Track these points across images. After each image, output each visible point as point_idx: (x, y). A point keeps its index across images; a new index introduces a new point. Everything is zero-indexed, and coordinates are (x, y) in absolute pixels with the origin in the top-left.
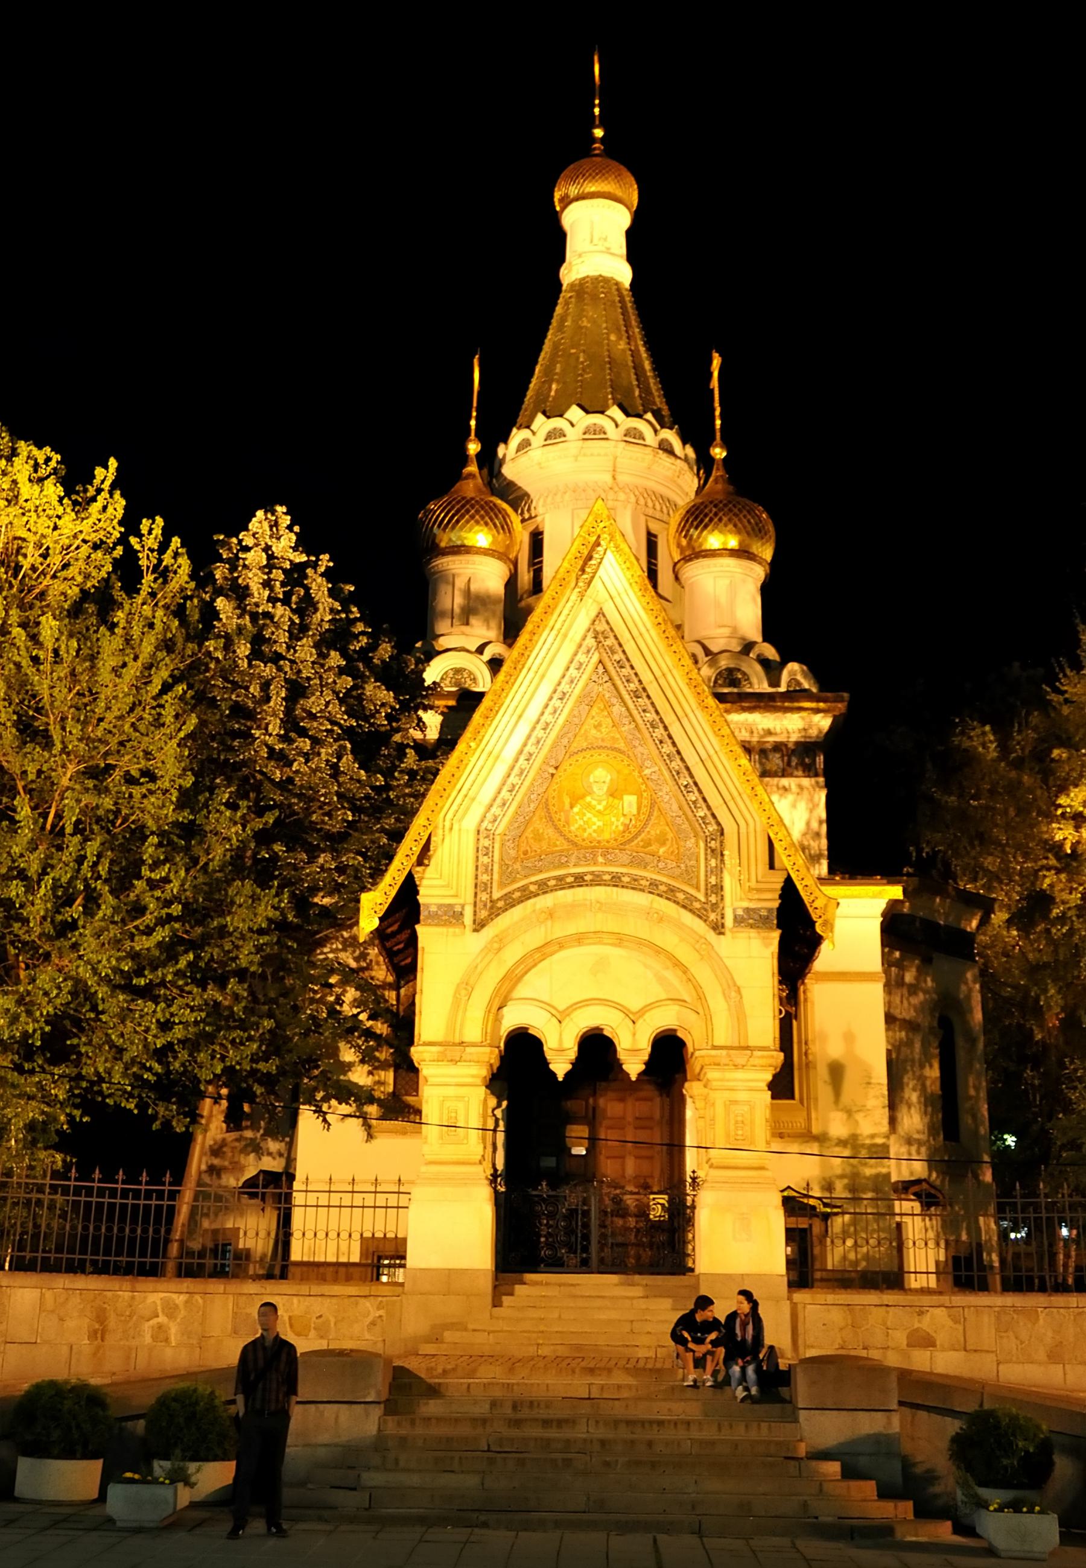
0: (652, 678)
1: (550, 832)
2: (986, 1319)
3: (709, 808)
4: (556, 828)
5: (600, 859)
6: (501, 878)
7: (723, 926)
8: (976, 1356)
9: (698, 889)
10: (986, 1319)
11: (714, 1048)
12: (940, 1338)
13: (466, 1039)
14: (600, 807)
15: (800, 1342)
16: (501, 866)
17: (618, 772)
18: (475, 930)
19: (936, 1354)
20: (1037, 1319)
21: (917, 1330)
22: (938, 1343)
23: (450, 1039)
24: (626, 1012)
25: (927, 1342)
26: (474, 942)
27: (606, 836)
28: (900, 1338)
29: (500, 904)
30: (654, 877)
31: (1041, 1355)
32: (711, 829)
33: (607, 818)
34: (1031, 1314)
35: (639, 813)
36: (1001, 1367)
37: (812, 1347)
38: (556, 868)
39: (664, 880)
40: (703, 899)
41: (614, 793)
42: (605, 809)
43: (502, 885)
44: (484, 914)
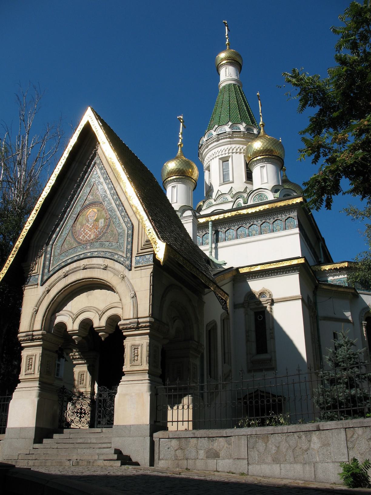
0: (110, 170)
1: (72, 241)
2: (243, 442)
3: (129, 218)
4: (75, 239)
5: (88, 247)
6: (53, 262)
7: (131, 266)
8: (238, 462)
9: (123, 252)
10: (243, 442)
11: (124, 320)
12: (222, 454)
13: (34, 329)
14: (91, 227)
15: (156, 457)
16: (54, 258)
17: (98, 211)
18: (42, 285)
19: (219, 461)
20: (268, 441)
21: (210, 450)
22: (221, 455)
23: (28, 330)
24: (97, 310)
25: (216, 455)
26: (41, 290)
27: (92, 237)
28: (202, 453)
29: (51, 273)
30: (107, 250)
31: (269, 459)
32: (129, 225)
33: (93, 230)
34: (266, 437)
35: (104, 226)
36: (250, 467)
37: (162, 459)
38: (72, 254)
39: (110, 251)
40: (125, 256)
41: (97, 220)
42: (93, 226)
43: (53, 266)
44: (45, 278)
